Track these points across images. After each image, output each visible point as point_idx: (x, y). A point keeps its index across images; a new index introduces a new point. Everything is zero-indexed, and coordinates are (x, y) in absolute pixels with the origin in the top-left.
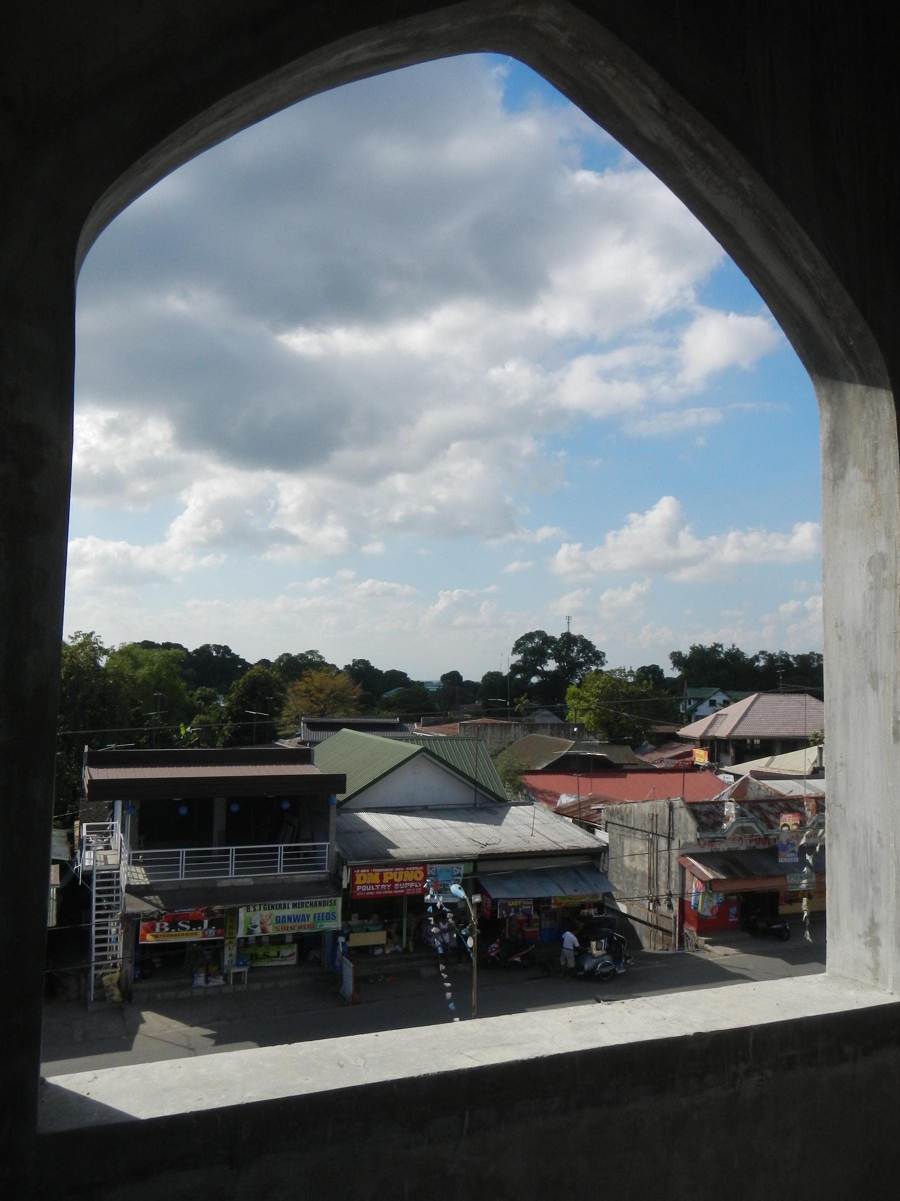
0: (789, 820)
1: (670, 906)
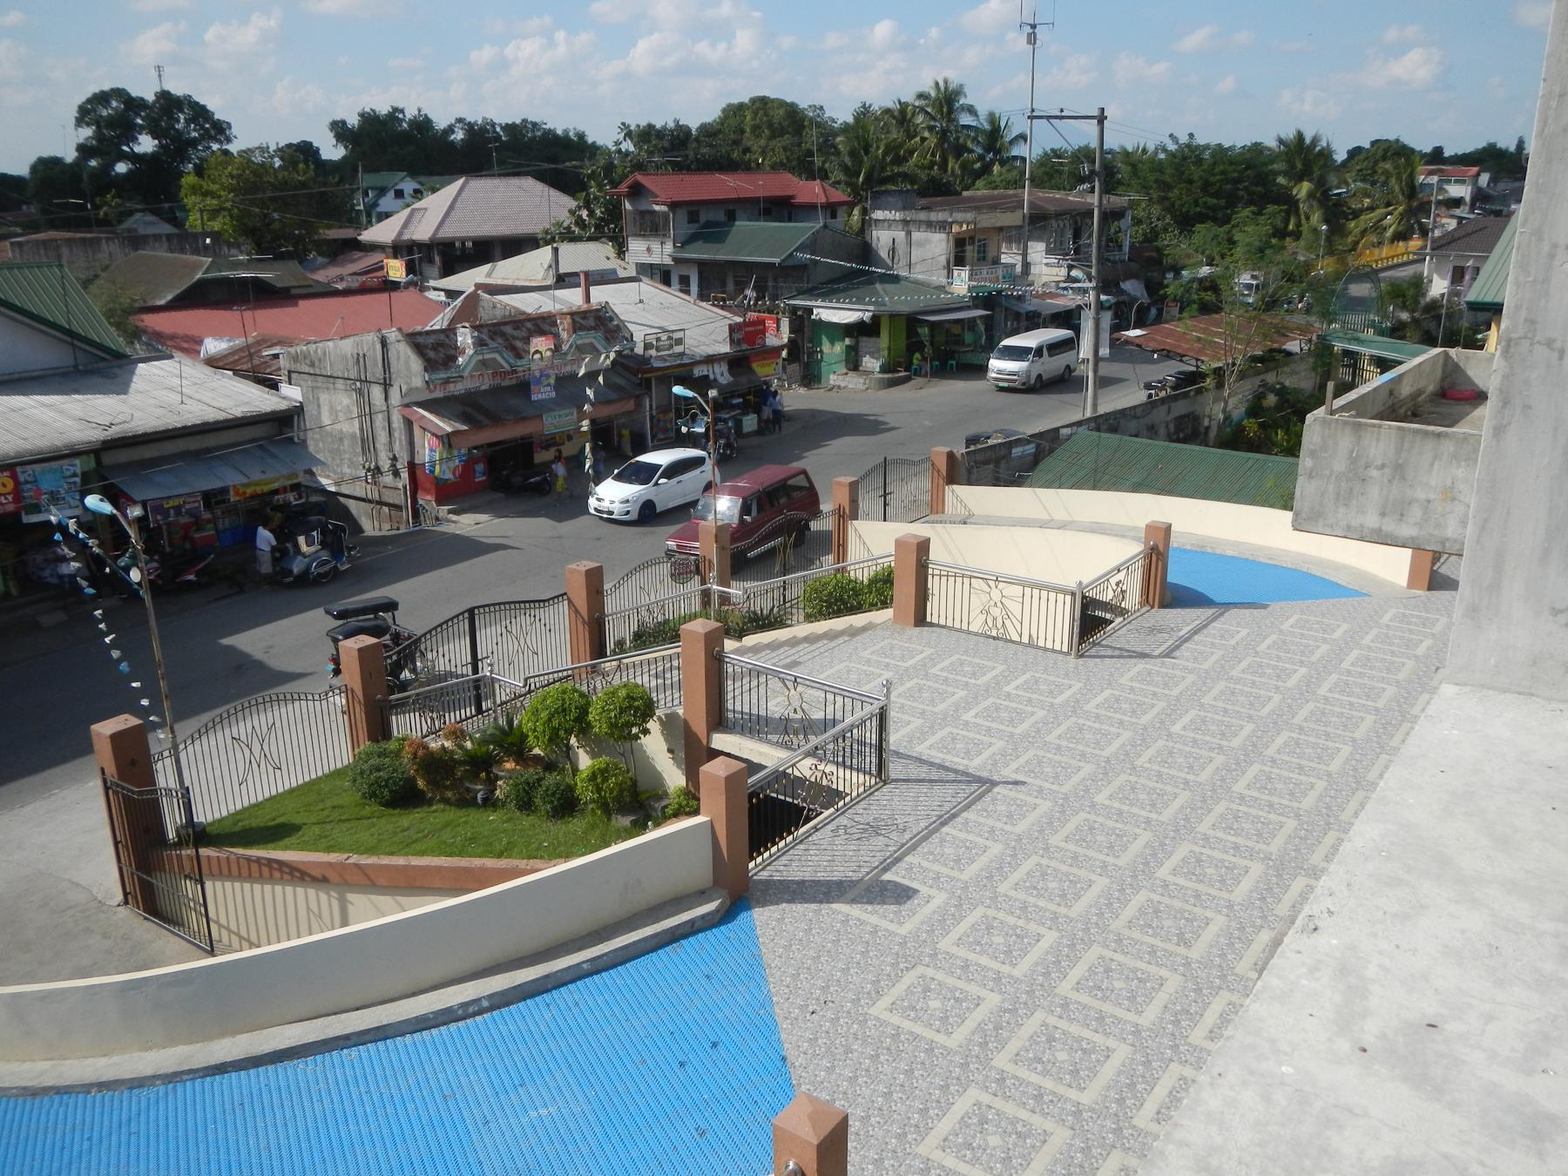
0: (541, 344)
1: (396, 474)
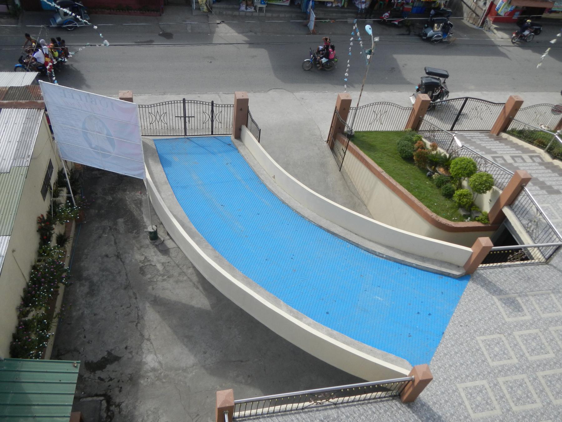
1: (485, 4)
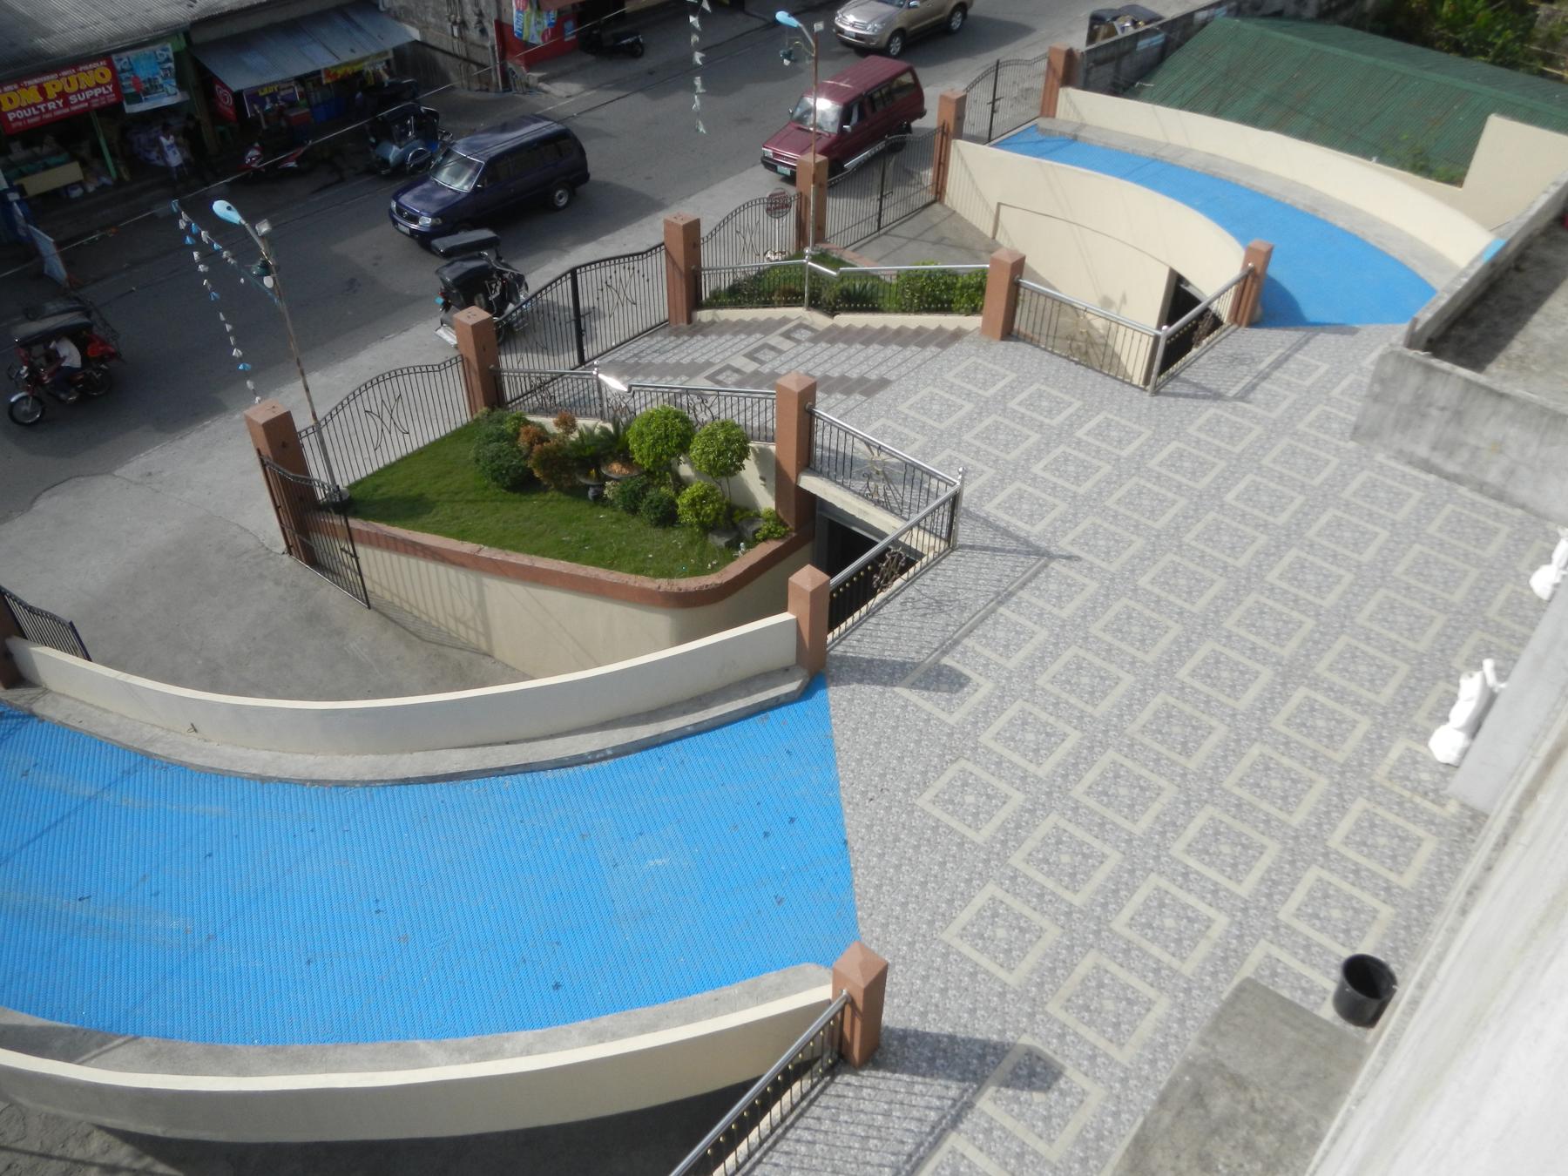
1: (483, 31)
